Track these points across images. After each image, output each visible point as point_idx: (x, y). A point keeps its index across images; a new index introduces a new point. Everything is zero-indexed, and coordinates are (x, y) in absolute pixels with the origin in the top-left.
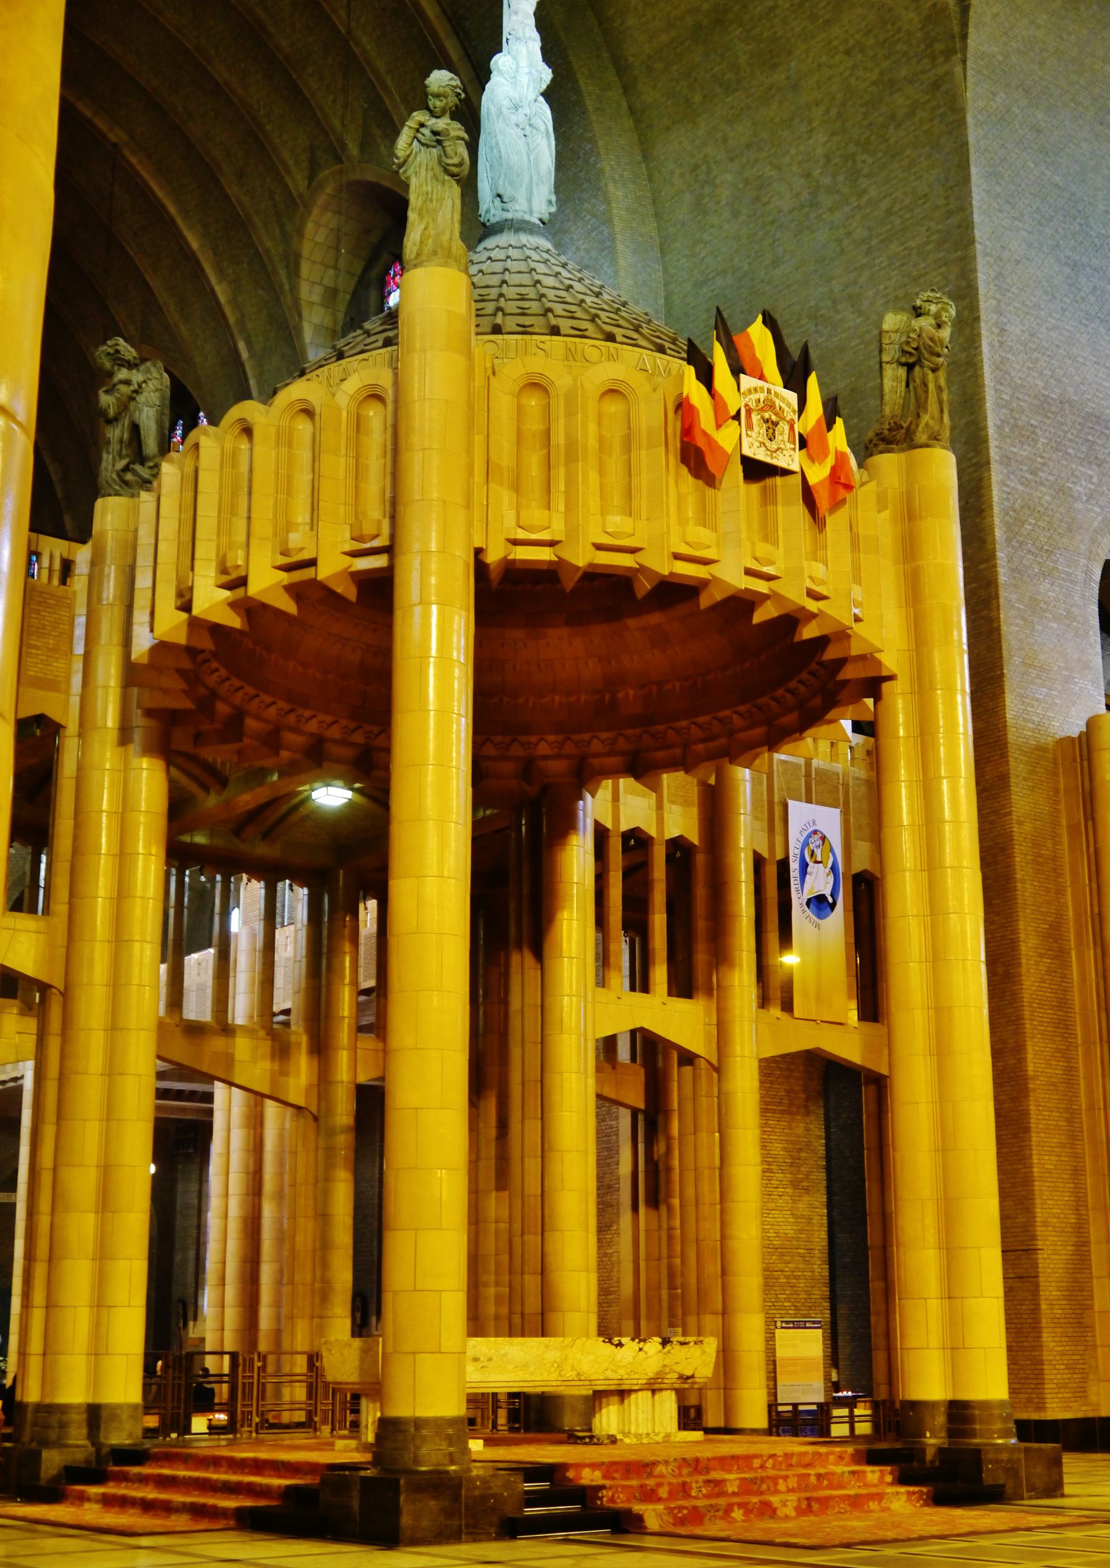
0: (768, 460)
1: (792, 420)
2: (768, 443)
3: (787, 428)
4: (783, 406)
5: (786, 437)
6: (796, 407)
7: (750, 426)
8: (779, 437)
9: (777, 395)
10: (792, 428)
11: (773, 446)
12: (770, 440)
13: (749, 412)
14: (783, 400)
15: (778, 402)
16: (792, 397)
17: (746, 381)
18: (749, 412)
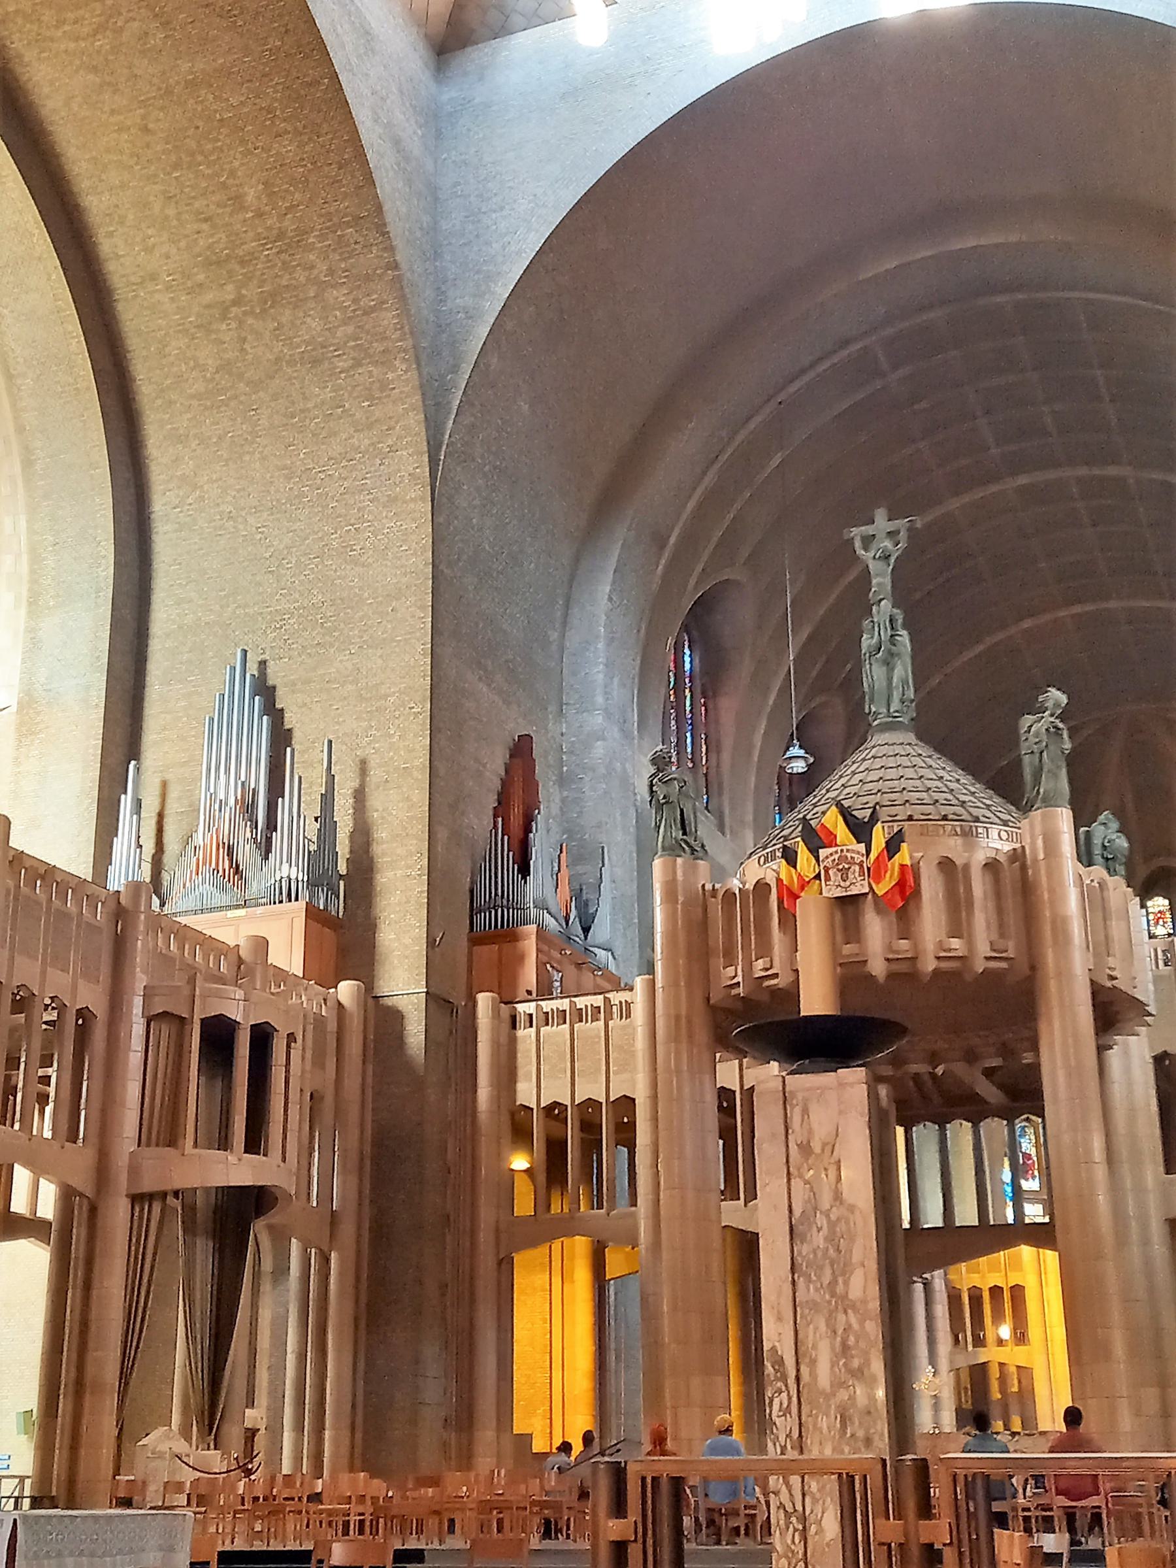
0: (844, 894)
1: (862, 861)
2: (842, 884)
3: (857, 868)
4: (853, 855)
5: (857, 874)
6: (864, 852)
7: (828, 879)
8: (851, 876)
9: (848, 851)
10: (861, 865)
11: (848, 883)
12: (845, 881)
13: (827, 870)
14: (853, 851)
15: (849, 855)
16: (862, 847)
17: (823, 853)
18: (827, 870)
